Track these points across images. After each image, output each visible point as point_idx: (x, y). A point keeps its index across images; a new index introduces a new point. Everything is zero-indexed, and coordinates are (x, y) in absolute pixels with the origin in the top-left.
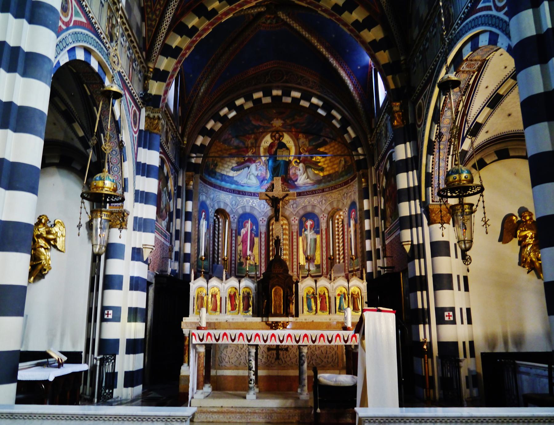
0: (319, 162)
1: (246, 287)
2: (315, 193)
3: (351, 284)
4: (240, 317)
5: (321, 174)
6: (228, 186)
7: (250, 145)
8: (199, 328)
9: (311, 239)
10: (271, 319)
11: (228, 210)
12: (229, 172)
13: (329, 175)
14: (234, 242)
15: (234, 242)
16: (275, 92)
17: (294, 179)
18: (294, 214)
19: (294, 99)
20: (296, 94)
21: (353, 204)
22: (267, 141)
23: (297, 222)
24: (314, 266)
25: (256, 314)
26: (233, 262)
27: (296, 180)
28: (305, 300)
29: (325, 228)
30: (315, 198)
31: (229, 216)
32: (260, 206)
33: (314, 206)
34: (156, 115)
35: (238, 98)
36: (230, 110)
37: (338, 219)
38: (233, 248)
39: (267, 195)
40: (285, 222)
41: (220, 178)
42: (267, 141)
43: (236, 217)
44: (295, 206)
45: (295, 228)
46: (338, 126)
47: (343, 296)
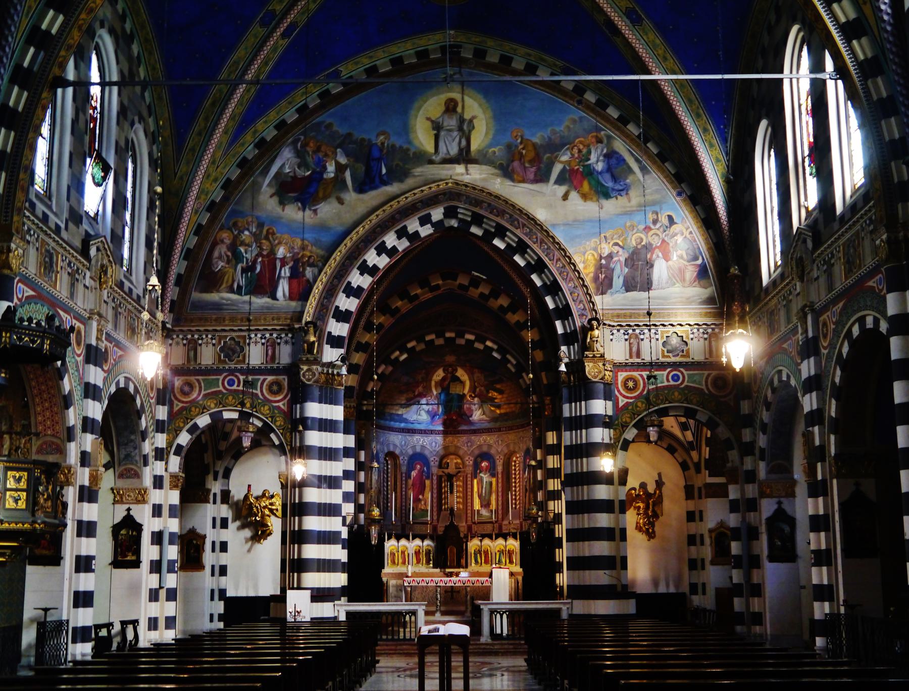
0: (496, 398)
1: (428, 545)
3: (507, 543)
4: (422, 569)
5: (498, 411)
6: (397, 425)
7: (420, 380)
8: (407, 577)
10: (448, 570)
11: (397, 452)
12: (398, 410)
13: (505, 414)
14: (404, 486)
15: (404, 486)
16: (448, 335)
17: (469, 414)
19: (468, 341)
20: (471, 337)
21: (527, 452)
22: (439, 374)
23: (471, 462)
25: (435, 567)
26: (404, 508)
27: (471, 416)
28: (473, 555)
30: (492, 437)
31: (398, 458)
33: (490, 446)
34: (352, 404)
36: (401, 354)
37: (515, 462)
38: (404, 493)
39: (443, 472)
40: (459, 461)
41: (389, 418)
42: (439, 374)
43: (406, 458)
44: (469, 444)
45: (469, 470)
46: (513, 370)
47: (501, 552)
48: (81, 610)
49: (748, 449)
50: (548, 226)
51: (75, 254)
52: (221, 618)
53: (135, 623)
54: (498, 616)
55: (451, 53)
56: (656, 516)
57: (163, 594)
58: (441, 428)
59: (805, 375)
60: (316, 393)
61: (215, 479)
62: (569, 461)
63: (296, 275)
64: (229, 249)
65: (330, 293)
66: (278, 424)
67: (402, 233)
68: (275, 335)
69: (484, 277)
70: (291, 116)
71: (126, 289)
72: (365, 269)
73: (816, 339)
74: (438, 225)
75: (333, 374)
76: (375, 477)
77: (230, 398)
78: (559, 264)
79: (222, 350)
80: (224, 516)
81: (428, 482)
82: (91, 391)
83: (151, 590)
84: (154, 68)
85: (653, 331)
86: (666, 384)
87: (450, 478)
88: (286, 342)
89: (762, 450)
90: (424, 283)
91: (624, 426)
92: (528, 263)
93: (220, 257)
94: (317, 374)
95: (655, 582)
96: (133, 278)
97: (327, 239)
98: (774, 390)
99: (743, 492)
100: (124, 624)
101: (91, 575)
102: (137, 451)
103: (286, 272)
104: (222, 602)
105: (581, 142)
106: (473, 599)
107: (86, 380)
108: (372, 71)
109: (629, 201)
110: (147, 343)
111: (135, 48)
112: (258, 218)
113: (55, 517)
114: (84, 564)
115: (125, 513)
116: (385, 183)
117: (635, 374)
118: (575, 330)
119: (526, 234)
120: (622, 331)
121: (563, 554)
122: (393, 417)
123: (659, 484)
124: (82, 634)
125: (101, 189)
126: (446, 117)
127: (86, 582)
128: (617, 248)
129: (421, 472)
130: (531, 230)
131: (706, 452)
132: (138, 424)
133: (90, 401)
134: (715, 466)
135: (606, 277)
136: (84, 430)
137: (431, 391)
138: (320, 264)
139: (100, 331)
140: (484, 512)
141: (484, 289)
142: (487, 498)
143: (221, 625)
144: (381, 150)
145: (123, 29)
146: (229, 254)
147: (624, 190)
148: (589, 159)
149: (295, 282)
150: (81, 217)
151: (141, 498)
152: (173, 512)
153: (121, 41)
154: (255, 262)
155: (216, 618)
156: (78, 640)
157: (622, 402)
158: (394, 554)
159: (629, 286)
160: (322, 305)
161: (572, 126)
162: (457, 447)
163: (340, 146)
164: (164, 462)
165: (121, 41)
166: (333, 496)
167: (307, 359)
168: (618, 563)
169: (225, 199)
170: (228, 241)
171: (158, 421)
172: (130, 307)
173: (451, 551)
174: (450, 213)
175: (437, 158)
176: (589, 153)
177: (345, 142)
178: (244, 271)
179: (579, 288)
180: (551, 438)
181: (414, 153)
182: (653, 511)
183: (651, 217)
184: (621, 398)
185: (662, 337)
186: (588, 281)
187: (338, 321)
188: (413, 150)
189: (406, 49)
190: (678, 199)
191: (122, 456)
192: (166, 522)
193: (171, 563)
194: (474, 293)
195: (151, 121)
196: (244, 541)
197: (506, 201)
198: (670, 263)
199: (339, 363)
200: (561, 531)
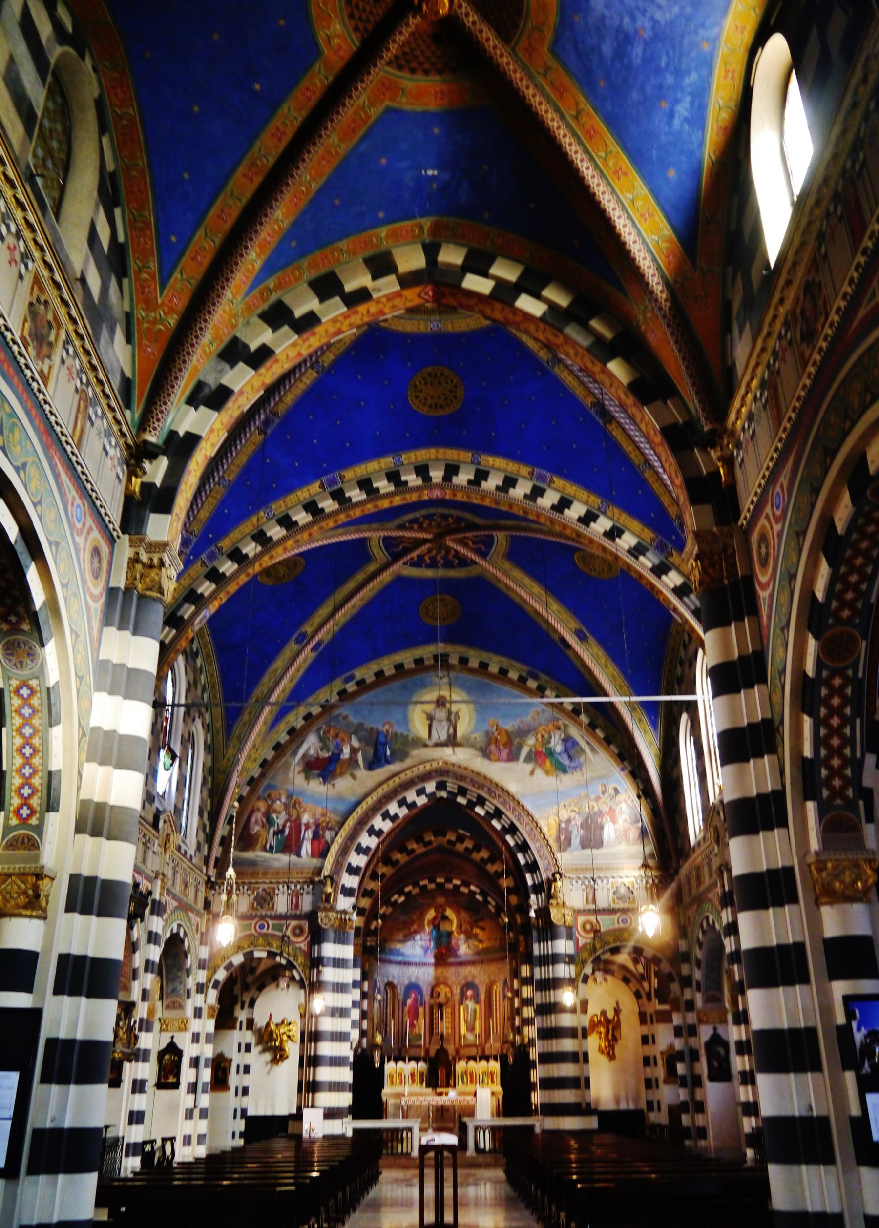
5: (481, 946)
10: (439, 1090)
11: (395, 982)
16: (440, 880)
20: (457, 882)
21: (505, 982)
22: (431, 914)
25: (428, 1086)
32: (424, 975)
33: (474, 977)
35: (407, 885)
36: (400, 896)
40: (448, 990)
42: (431, 914)
43: (403, 988)
45: (457, 997)
46: (493, 910)
47: (484, 1073)
48: (134, 1127)
49: (686, 982)
50: (518, 797)
51: (149, 827)
52: (242, 1135)
53: (172, 1139)
54: (482, 1132)
55: (442, 661)
56: (615, 1039)
57: (196, 1113)
58: (432, 960)
59: (725, 922)
60: (331, 935)
61: (242, 1008)
62: (539, 993)
63: (316, 836)
64: (263, 815)
65: (344, 851)
66: (299, 961)
67: (402, 803)
68: (299, 887)
69: (468, 834)
70: (316, 710)
71: (183, 851)
72: (372, 832)
73: (731, 892)
74: (431, 796)
75: (345, 919)
76: (376, 1005)
77: (261, 940)
78: (528, 828)
79: (255, 899)
80: (248, 1040)
81: (421, 1010)
82: (153, 938)
83: (187, 1110)
84: (212, 676)
85: (605, 881)
86: (616, 926)
87: (440, 1006)
88: (308, 893)
89: (698, 983)
90: (419, 840)
91: (584, 963)
92: (503, 827)
93: (257, 822)
94: (332, 920)
95: (617, 1101)
96: (188, 841)
97: (342, 807)
98: (704, 932)
99: (684, 1018)
100: (164, 1140)
101: (144, 1096)
102: (182, 986)
103: (309, 834)
104: (243, 1121)
105: (544, 730)
106: (460, 1117)
107: (150, 929)
108: (379, 674)
109: (583, 775)
110: (224, 917)
111: (199, 662)
112: (287, 790)
113: (129, 1047)
114: (138, 1086)
115: (169, 1040)
116: (388, 762)
117: (592, 918)
118: (542, 881)
119: (501, 804)
120: (580, 882)
121: (536, 1075)
122: (392, 952)
123: (617, 1011)
124: (135, 1149)
125: (169, 773)
126: (438, 711)
127: (140, 1102)
128: (573, 815)
129: (415, 1000)
130: (505, 800)
131: (655, 982)
132: (184, 963)
133: (152, 946)
134: (662, 995)
135: (566, 838)
136: (146, 970)
137: (424, 927)
138: (337, 828)
139: (162, 888)
140: (470, 1037)
141: (469, 844)
143: (240, 1142)
144: (386, 737)
145: (192, 649)
146: (264, 820)
147: (579, 767)
148: (549, 742)
149: (316, 843)
150: (154, 798)
151: (183, 1026)
152: (209, 1039)
153: (189, 658)
154: (284, 826)
155: (237, 1135)
156: (131, 1153)
157: (582, 942)
158: (392, 1076)
159: (584, 845)
160: (338, 861)
161: (536, 717)
162: (446, 978)
163: (355, 733)
164: (203, 995)
165: (189, 658)
166: (343, 1025)
167: (325, 907)
168: (581, 1083)
169: (263, 775)
170: (263, 809)
171: (200, 960)
172: (184, 865)
173: (442, 1073)
174: (441, 786)
175: (430, 743)
176: (550, 737)
177: (358, 730)
178: (275, 833)
179: (545, 848)
180: (525, 971)
181: (413, 739)
182: (613, 1035)
183: (600, 789)
184: (580, 939)
185: (613, 887)
186: (551, 842)
187: (350, 874)
188: (411, 736)
189: (406, 657)
190: (622, 773)
191: (169, 991)
192: (202, 1048)
193: (205, 1085)
194: (460, 847)
195: (207, 716)
196: (264, 1064)
197: (485, 778)
198: (617, 826)
199: (351, 910)
200: (534, 1054)
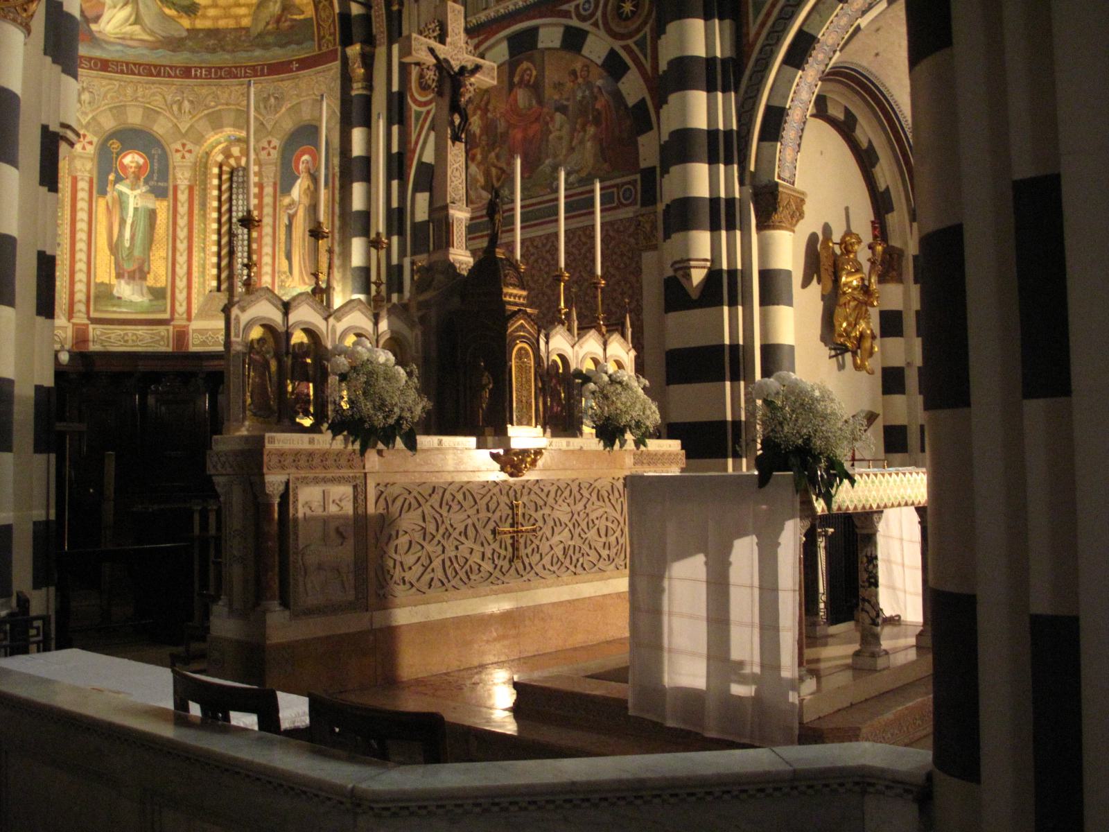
2: (158, 75)
5: (186, 23)
9: (136, 209)
13: (213, 33)
18: (84, 122)
24: (145, 290)
27: (97, 19)
29: (186, 183)
30: (154, 89)
140: (125, 290)
142: (137, 252)
